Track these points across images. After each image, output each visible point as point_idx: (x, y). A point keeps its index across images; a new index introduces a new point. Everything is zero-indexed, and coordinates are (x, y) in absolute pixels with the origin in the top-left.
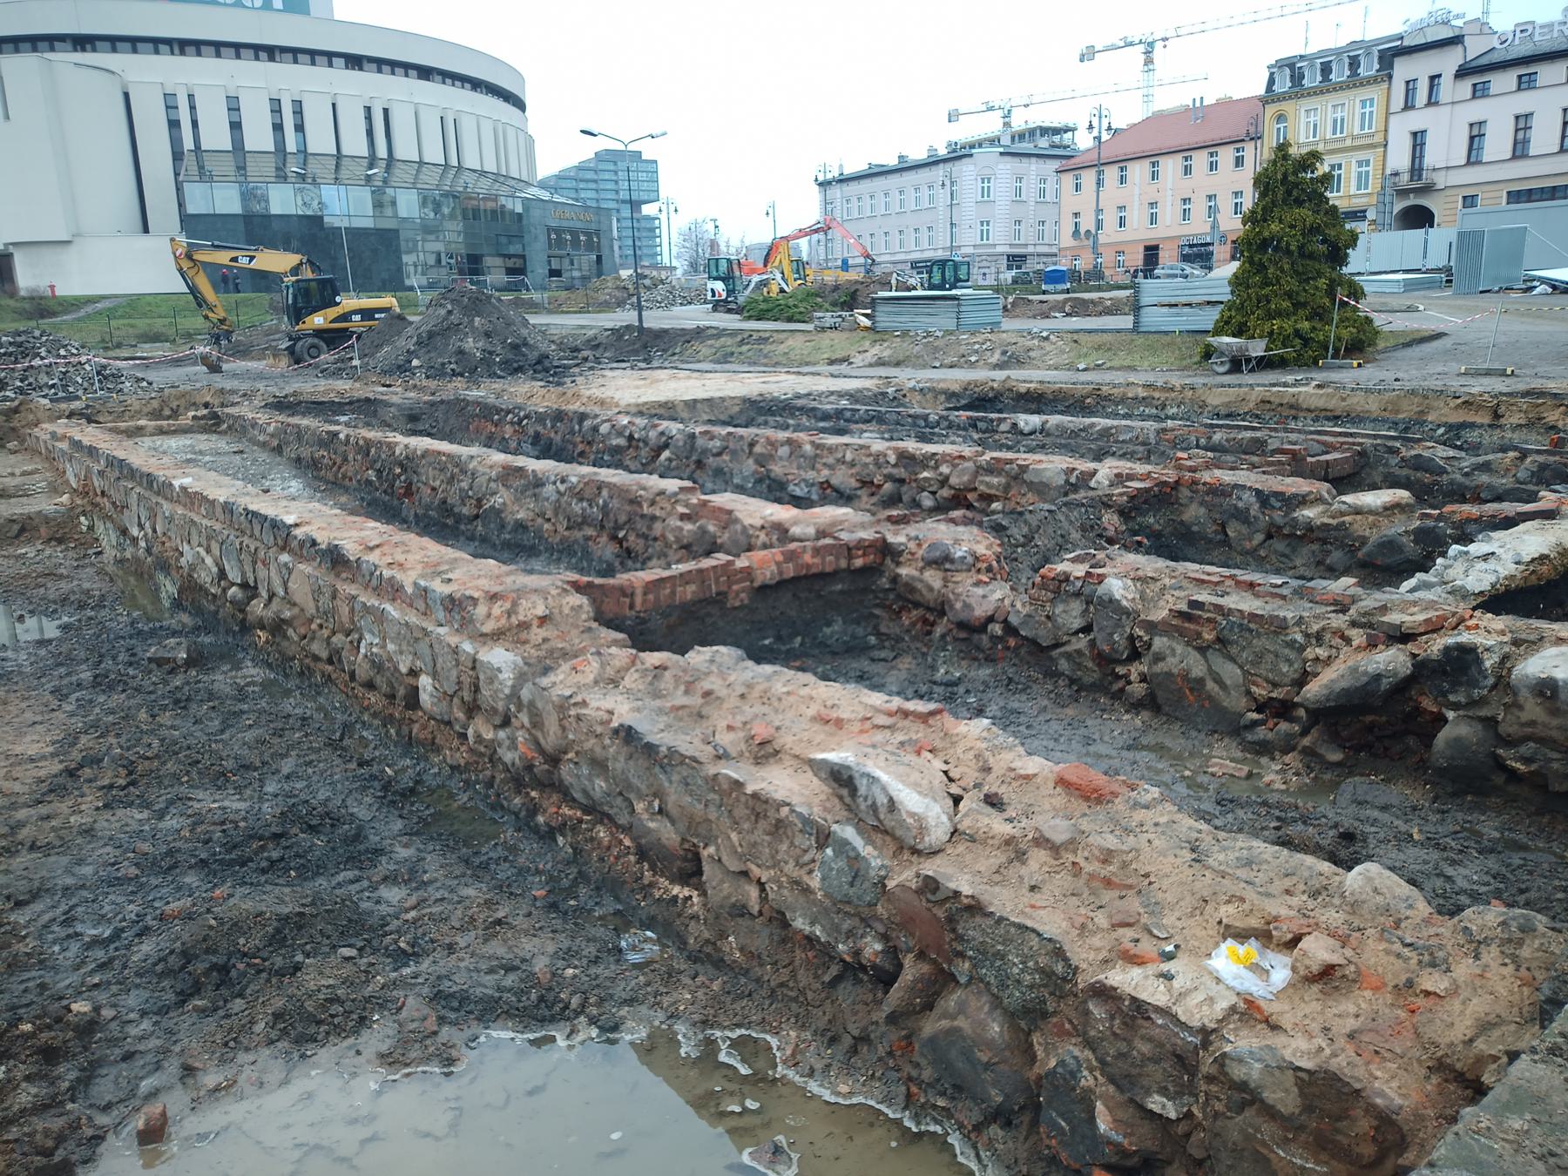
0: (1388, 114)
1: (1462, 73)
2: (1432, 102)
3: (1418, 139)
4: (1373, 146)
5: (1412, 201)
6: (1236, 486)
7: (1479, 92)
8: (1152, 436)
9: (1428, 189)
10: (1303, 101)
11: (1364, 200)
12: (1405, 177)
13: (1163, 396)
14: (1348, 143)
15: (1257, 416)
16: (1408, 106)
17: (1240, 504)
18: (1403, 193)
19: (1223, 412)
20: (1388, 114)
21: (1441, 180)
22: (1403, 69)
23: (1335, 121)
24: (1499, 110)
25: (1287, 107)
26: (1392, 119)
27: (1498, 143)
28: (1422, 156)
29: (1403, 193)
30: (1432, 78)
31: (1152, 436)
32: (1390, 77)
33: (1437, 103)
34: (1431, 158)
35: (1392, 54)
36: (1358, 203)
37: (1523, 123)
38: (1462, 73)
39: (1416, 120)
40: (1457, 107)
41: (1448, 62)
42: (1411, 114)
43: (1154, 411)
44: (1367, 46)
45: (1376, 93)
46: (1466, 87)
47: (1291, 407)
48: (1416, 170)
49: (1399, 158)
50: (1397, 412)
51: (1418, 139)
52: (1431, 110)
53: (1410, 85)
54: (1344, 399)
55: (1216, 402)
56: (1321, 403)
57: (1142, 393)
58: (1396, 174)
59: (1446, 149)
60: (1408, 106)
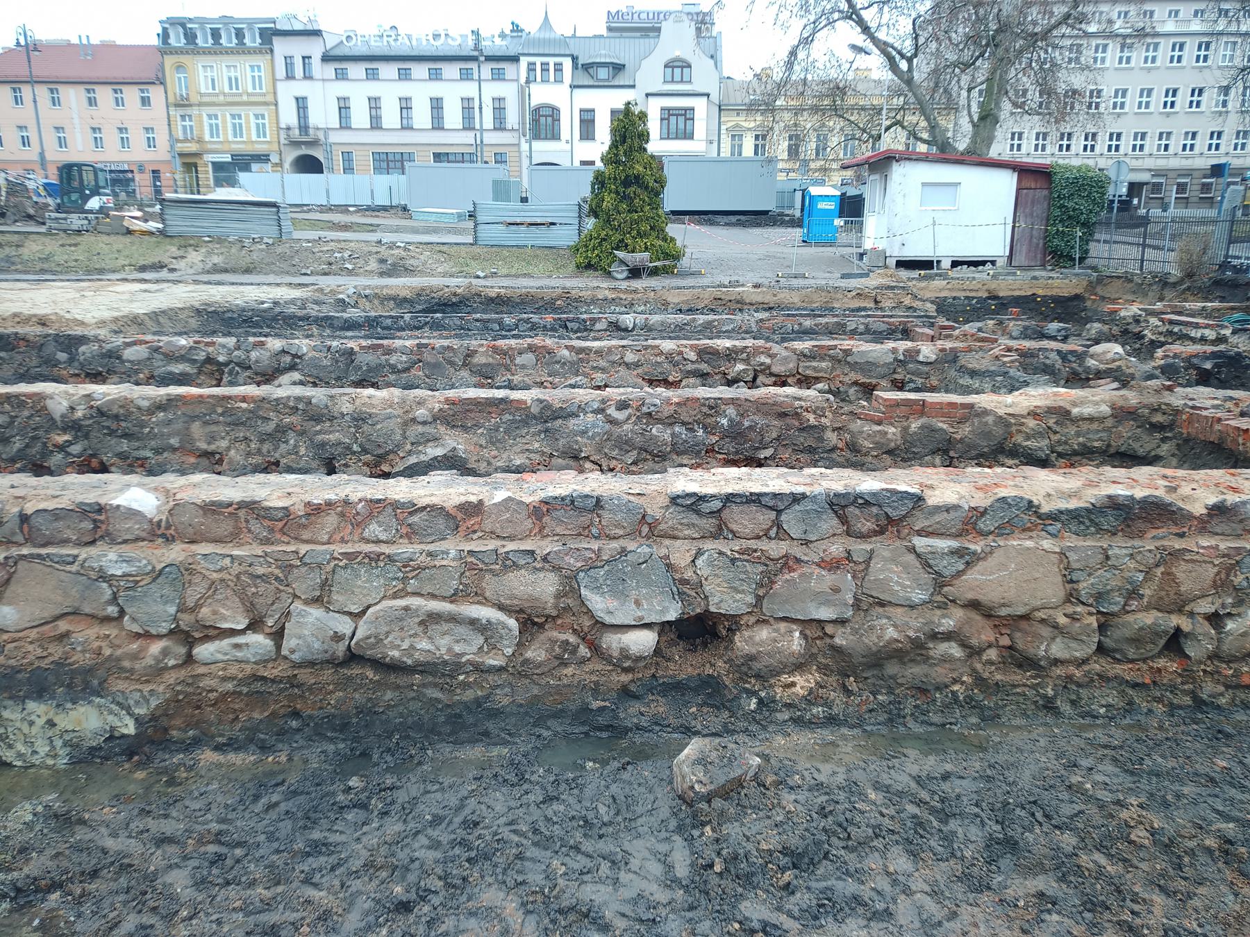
0: (275, 80)
1: (326, 58)
2: (308, 77)
4: (266, 104)
5: (304, 151)
6: (1040, 349)
8: (753, 325)
9: (314, 143)
10: (198, 57)
11: (265, 146)
12: (297, 132)
13: (630, 297)
14: (245, 98)
15: (712, 310)
17: (1048, 362)
18: (295, 144)
19: (685, 308)
20: (275, 80)
22: (281, 47)
23: (230, 79)
25: (183, 59)
26: (280, 85)
27: (360, 116)
28: (306, 117)
29: (295, 144)
30: (304, 58)
31: (753, 325)
32: (272, 51)
33: (311, 78)
35: (270, 34)
36: (260, 148)
37: (374, 104)
38: (326, 58)
40: (328, 84)
41: (315, 49)
42: (292, 83)
43: (623, 309)
44: (251, 22)
45: (262, 61)
47: (738, 302)
48: (304, 128)
49: (289, 116)
50: (812, 302)
52: (307, 83)
53: (289, 61)
54: (775, 295)
55: (676, 300)
56: (759, 299)
57: (611, 295)
58: (288, 129)
59: (322, 116)
60: (290, 77)
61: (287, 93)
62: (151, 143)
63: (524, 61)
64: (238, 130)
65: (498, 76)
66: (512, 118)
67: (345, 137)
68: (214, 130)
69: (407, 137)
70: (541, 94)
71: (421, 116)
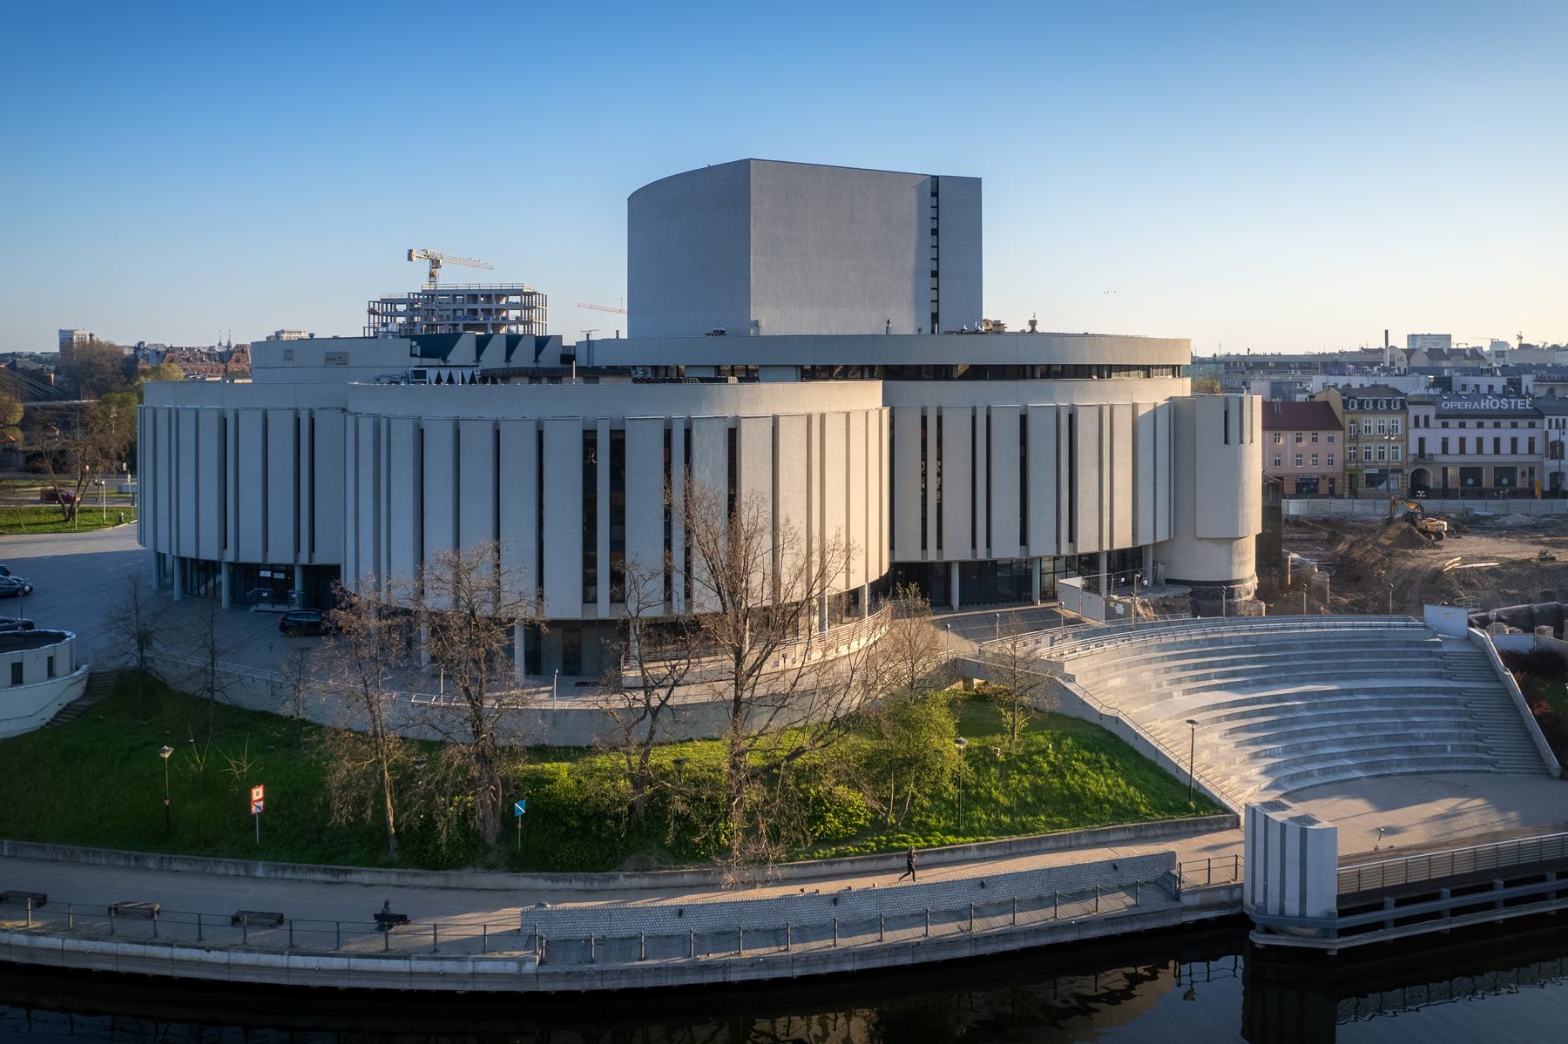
1: (1438, 417)
3: (1422, 441)
7: (1445, 425)
16: (1417, 425)
21: (1437, 459)
24: (1454, 434)
26: (1411, 432)
27: (1454, 447)
34: (1428, 451)
38: (1438, 417)
39: (1422, 432)
46: (1439, 422)
49: (1414, 448)
51: (1422, 441)
53: (1417, 419)
59: (1433, 447)
61: (1414, 435)
62: (1331, 463)
63: (1547, 419)
64: (1382, 455)
65: (1532, 425)
66: (1539, 447)
67: (1445, 458)
68: (1368, 455)
69: (1480, 458)
70: (1554, 435)
71: (1488, 447)
